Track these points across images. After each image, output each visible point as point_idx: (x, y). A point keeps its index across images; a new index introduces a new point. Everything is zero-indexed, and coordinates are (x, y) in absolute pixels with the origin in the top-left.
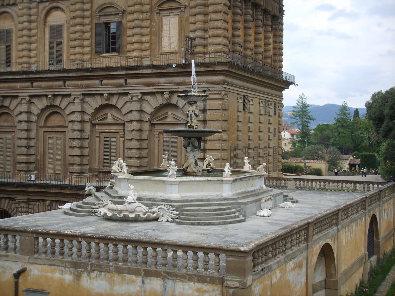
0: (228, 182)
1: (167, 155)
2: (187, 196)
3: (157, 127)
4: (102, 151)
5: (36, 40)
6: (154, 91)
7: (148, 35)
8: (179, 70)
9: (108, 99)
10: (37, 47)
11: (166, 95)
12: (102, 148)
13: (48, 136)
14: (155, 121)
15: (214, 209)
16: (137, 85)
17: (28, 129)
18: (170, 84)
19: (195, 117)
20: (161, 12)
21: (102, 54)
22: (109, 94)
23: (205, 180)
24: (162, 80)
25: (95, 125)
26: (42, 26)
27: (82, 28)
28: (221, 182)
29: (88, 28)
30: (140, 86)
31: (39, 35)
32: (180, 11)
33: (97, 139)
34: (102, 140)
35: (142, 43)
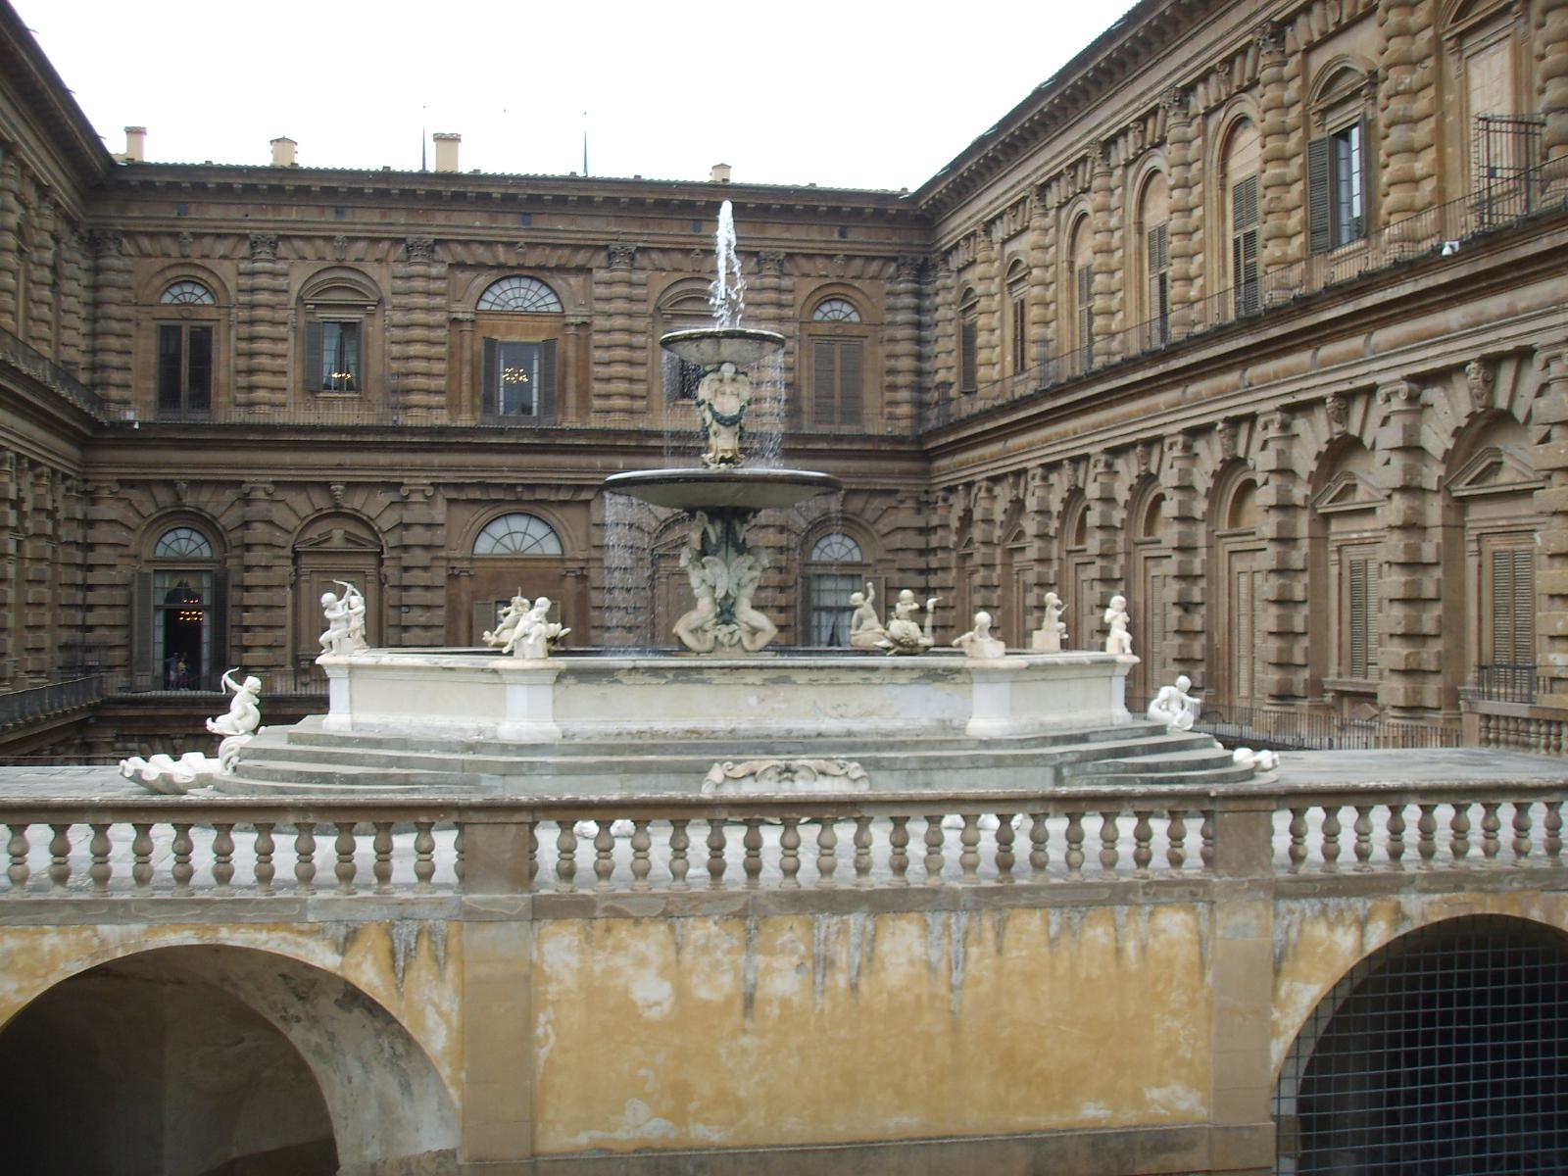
0: (519, 678)
1: (872, 592)
2: (372, 725)
3: (1478, 514)
4: (1346, 616)
5: (1202, 241)
6: (1439, 364)
7: (1430, 146)
8: (1485, 264)
9: (1342, 416)
10: (1202, 265)
12: (1346, 602)
13: (1240, 564)
14: (1461, 486)
15: (300, 773)
16: (1397, 348)
17: (1185, 544)
18: (1475, 327)
19: (715, 426)
20: (1468, 43)
21: (1331, 251)
22: (1338, 395)
23: (427, 664)
24: (1454, 317)
26: (1214, 192)
27: (1278, 171)
28: (494, 678)
29: (1293, 169)
31: (1208, 224)
32: (1510, 20)
33: (1334, 570)
34: (1346, 573)
35: (1415, 182)
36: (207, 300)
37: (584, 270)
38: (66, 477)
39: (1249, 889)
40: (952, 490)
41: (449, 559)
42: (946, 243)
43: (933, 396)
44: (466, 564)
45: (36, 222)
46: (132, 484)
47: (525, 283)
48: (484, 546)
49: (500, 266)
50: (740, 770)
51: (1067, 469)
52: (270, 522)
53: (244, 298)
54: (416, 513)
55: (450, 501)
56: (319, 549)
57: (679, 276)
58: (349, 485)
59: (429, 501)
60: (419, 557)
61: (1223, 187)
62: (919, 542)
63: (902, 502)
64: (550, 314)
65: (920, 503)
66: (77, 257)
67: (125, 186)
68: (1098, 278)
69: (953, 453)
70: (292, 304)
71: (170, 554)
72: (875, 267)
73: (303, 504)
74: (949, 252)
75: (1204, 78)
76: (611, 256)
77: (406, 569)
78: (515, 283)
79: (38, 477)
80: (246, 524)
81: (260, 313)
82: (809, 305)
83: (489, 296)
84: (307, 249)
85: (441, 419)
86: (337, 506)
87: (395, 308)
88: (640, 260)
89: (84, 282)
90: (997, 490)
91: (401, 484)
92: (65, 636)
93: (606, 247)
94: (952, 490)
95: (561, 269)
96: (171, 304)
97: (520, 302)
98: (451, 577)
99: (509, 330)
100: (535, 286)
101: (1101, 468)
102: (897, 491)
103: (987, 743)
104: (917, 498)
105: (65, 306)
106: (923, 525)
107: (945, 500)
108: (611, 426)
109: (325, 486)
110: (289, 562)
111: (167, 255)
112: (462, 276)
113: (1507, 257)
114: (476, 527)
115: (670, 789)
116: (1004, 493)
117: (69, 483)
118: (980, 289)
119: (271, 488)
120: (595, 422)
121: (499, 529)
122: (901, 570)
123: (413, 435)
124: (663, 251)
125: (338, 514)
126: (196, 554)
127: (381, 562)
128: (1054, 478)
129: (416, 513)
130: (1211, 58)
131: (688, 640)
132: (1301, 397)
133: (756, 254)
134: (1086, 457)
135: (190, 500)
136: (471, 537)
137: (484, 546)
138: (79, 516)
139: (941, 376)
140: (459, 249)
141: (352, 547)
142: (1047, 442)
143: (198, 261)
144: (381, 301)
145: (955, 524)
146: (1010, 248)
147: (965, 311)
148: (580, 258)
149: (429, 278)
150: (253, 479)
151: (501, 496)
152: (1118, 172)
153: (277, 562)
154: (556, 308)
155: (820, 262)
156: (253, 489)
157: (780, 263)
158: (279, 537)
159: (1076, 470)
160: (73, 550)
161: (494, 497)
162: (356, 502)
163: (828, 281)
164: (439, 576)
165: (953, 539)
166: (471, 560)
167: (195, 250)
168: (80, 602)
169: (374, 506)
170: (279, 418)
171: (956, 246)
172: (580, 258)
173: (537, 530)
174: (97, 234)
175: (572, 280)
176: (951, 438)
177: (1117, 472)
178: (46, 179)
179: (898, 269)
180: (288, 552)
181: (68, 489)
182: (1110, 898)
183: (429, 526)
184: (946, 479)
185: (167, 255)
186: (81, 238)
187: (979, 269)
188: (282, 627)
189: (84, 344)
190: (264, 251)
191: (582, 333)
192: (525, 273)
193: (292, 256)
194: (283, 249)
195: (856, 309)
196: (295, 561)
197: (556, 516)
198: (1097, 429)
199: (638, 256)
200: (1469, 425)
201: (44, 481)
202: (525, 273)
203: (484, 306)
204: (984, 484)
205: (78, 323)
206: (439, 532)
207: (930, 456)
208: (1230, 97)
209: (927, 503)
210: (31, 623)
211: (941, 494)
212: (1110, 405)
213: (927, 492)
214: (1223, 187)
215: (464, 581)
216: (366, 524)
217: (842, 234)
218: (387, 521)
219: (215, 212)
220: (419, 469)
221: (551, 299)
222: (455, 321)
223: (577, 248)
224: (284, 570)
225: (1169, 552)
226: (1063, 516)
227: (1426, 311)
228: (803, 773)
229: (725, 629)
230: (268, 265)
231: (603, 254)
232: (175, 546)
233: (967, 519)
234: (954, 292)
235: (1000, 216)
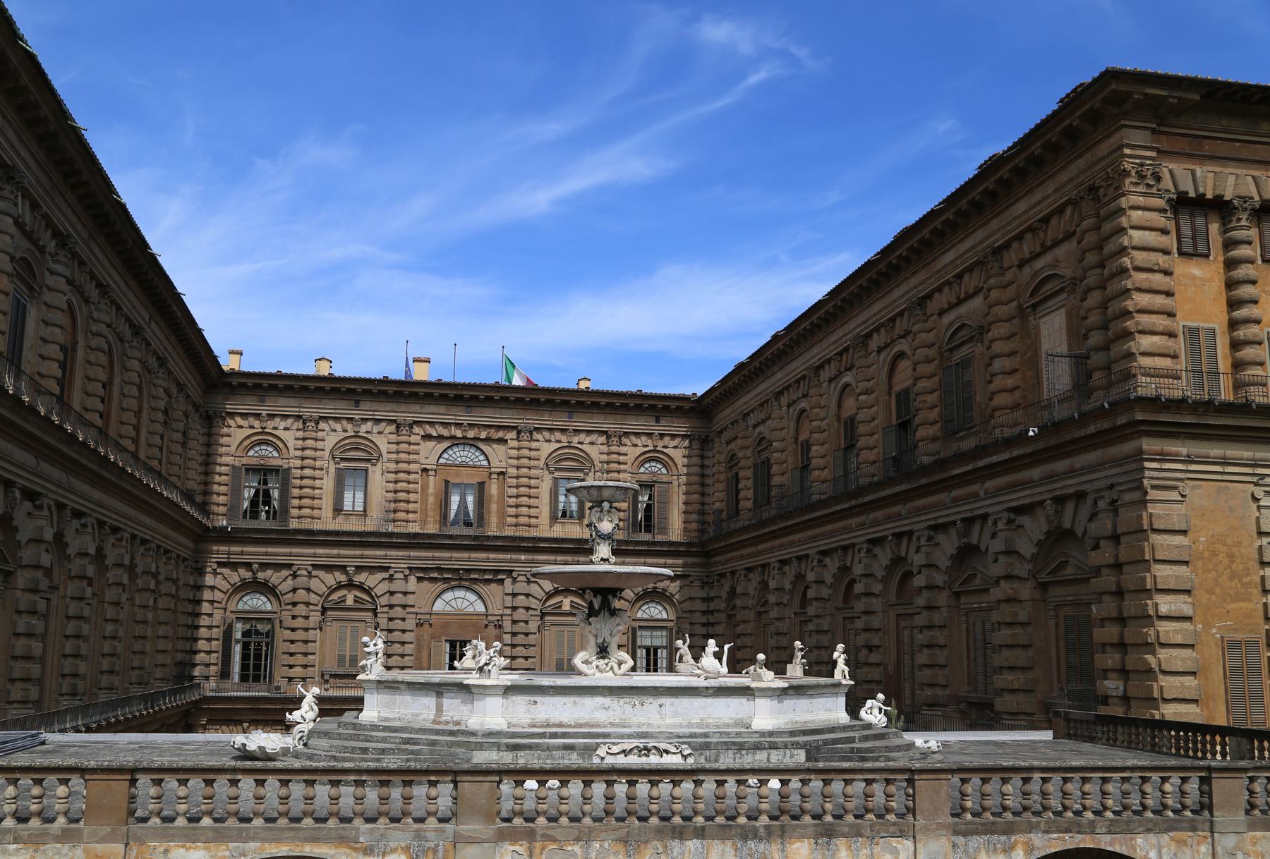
6: (1027, 501)
9: (967, 532)
11: (1050, 508)
13: (903, 624)
16: (1000, 490)
17: (869, 610)
22: (963, 520)
24: (1035, 473)
25: (957, 595)
30: (1007, 493)
36: (275, 454)
37: (502, 441)
38: (185, 560)
39: (937, 829)
40: (722, 575)
41: (417, 614)
42: (717, 427)
43: (710, 519)
44: (427, 617)
45: (175, 406)
47: (467, 448)
48: (439, 606)
49: (453, 437)
50: (615, 749)
51: (795, 563)
52: (308, 590)
53: (299, 453)
54: (398, 585)
55: (420, 579)
56: (340, 606)
57: (560, 445)
58: (357, 567)
59: (406, 578)
60: (398, 612)
61: (890, 394)
62: (703, 607)
63: (692, 582)
64: (483, 467)
65: (703, 582)
66: (199, 427)
67: (229, 385)
68: (814, 448)
69: (723, 553)
70: (326, 458)
71: (247, 608)
72: (676, 442)
73: (330, 579)
74: (721, 432)
75: (877, 330)
76: (519, 433)
77: (391, 619)
78: (461, 447)
79: (169, 559)
80: (294, 590)
81: (307, 462)
82: (637, 463)
83: (445, 456)
84: (338, 426)
85: (414, 528)
86: (350, 580)
87: (389, 461)
88: (536, 436)
89: (201, 442)
90: (751, 576)
91: (390, 567)
92: (179, 656)
93: (516, 427)
94: (722, 575)
95: (488, 440)
96: (253, 456)
97: (464, 459)
98: (419, 625)
99: (457, 475)
100: (473, 450)
101: (815, 563)
102: (689, 576)
103: (771, 734)
104: (701, 580)
105: (190, 456)
106: (705, 596)
107: (718, 581)
108: (518, 534)
109: (343, 568)
110: (319, 614)
111: (345, 431)
112: (431, 444)
113: (1068, 437)
114: (435, 593)
115: (574, 760)
116: (755, 578)
117: (186, 563)
118: (740, 455)
119: (310, 568)
120: (509, 532)
121: (448, 596)
122: (691, 624)
123: (398, 538)
124: (550, 430)
125: (350, 585)
126: (263, 608)
127: (376, 615)
128: (786, 568)
129: (398, 585)
130: (881, 318)
131: (583, 668)
132: (940, 521)
133: (606, 432)
134: (807, 556)
135: (261, 576)
136: (431, 600)
137: (439, 606)
138: (192, 583)
139: (717, 505)
140: (427, 427)
142: (782, 546)
144: (381, 455)
145: (724, 596)
146: (758, 430)
147: (730, 467)
148: (500, 434)
149: (409, 444)
151: (450, 576)
152: (825, 385)
153: (311, 614)
154: (485, 463)
155: (643, 438)
156: (299, 569)
157: (620, 437)
158: (313, 598)
159: (799, 564)
160: (187, 603)
161: (445, 576)
162: (360, 578)
163: (648, 449)
164: (410, 623)
165: (722, 606)
166: (431, 614)
167: (270, 425)
168: (189, 636)
169: (370, 580)
170: (317, 526)
171: (725, 429)
172: (500, 434)
173: (472, 597)
174: (210, 413)
175: (495, 446)
176: (722, 544)
177: (826, 566)
178: (182, 379)
179: (690, 442)
180: (319, 608)
181: (186, 567)
182: (848, 833)
183: (405, 593)
184: (720, 569)
185: (252, 427)
186: (201, 416)
187: (739, 442)
188: (314, 654)
189: (199, 478)
190: (525, 436)
191: (501, 477)
192: (467, 442)
193: (542, 439)
194: (322, 425)
195: (665, 466)
196: (323, 613)
197: (482, 588)
198: (814, 538)
199: (534, 433)
200: (1046, 539)
201: (173, 562)
202: (467, 442)
203: (442, 461)
204: (743, 572)
205: (197, 466)
206: (411, 596)
207: (707, 554)
208: (893, 341)
209: (708, 583)
210: (159, 648)
211: (716, 578)
212: (820, 525)
213: (707, 576)
214: (890, 394)
215: (426, 626)
216: (368, 591)
217: (657, 420)
218: (379, 590)
220: (399, 559)
221: (482, 458)
222: (425, 470)
223: (499, 428)
224: (315, 618)
225: (859, 615)
226: (791, 592)
227: (1018, 469)
228: (653, 751)
229: (601, 661)
230: (314, 435)
231: (515, 432)
232: (250, 603)
233: (732, 593)
234: (724, 455)
235: (752, 411)
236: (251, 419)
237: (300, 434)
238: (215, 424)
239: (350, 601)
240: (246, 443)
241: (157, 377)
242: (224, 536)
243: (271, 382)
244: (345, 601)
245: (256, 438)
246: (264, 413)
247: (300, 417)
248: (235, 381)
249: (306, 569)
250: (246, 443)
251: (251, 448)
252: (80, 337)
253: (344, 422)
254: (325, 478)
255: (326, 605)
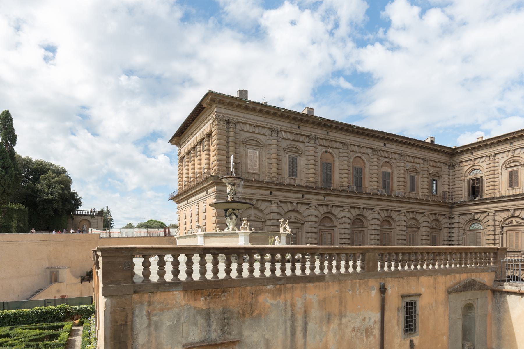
46: (463, 214)
67: (457, 153)
73: (504, 215)
125: (513, 216)
141: (518, 224)
143: (476, 164)
150: (489, 211)
219: (479, 152)
236: (469, 162)
237: (489, 162)
238: (456, 167)
239: (515, 223)
240: (468, 171)
241: (400, 160)
242: (461, 205)
243: (472, 147)
244: (512, 223)
245: (472, 168)
246: (473, 159)
247: (487, 156)
248: (459, 151)
249: (492, 213)
250: (468, 171)
251: (471, 172)
252: (336, 159)
253: (507, 153)
254: (500, 177)
255: (503, 225)
